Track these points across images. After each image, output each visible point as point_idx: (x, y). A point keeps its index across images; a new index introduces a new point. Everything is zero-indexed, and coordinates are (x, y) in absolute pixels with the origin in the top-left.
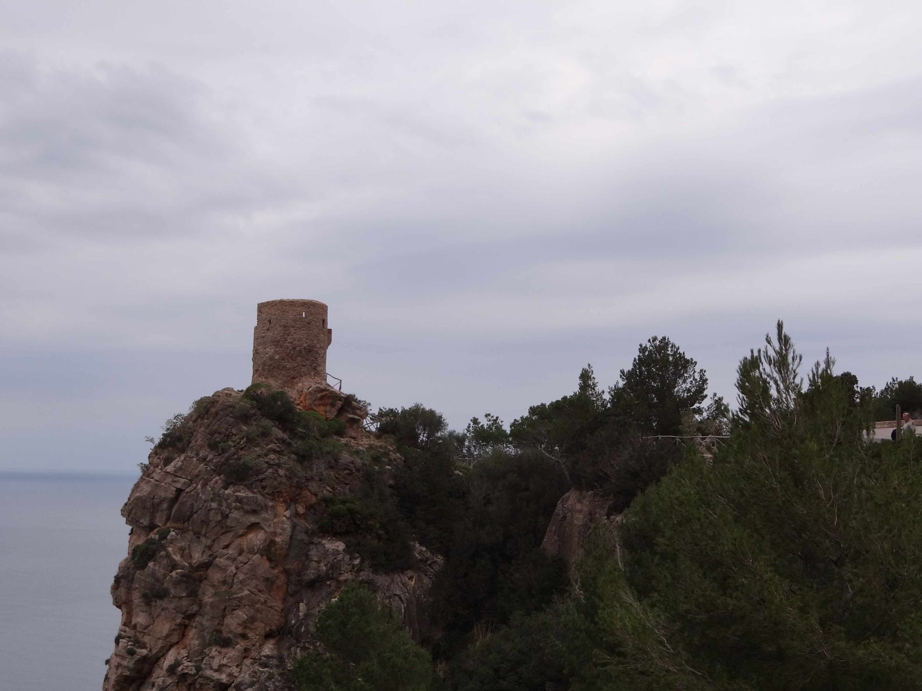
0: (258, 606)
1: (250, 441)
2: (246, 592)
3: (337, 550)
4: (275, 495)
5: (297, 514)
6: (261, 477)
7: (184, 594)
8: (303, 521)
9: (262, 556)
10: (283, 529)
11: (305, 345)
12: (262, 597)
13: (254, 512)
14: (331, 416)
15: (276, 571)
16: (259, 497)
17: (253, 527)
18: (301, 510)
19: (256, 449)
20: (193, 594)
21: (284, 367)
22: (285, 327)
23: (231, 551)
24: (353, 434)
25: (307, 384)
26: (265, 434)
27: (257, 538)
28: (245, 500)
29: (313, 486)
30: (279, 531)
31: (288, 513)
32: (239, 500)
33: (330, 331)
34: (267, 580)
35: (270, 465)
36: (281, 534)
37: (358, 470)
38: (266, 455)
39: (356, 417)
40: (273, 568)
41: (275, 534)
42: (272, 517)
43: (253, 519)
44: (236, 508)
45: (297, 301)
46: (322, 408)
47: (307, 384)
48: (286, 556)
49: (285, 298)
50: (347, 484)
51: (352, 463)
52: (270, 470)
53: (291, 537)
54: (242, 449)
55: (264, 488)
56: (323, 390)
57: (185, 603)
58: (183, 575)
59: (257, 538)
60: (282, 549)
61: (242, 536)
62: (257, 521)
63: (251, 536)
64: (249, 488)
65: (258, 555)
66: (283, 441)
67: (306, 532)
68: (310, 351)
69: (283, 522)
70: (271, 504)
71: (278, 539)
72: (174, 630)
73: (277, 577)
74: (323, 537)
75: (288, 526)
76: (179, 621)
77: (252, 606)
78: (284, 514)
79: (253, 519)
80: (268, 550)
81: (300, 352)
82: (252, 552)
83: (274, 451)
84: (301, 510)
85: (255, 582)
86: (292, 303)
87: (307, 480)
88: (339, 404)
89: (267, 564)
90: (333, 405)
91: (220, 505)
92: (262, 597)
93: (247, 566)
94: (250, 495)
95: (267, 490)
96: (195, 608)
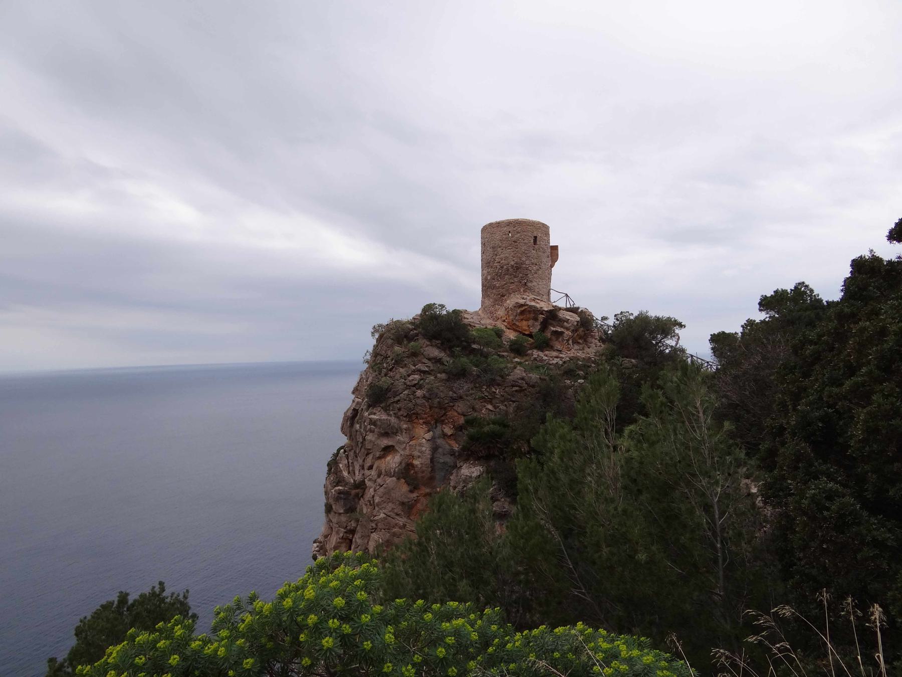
0: (396, 530)
1: (399, 362)
2: (382, 515)
3: (471, 477)
4: (412, 417)
5: (444, 435)
6: (396, 399)
7: (342, 511)
8: (452, 443)
9: (398, 479)
10: (421, 452)
11: (512, 263)
12: (401, 521)
13: (386, 434)
14: (536, 328)
15: (415, 495)
16: (393, 420)
17: (388, 450)
18: (448, 430)
19: (401, 370)
20: (350, 510)
21: (494, 287)
22: (493, 248)
23: (373, 472)
24: (559, 347)
25: (512, 301)
26: (414, 354)
27: (393, 461)
28: (378, 423)
29: (461, 406)
30: (416, 453)
31: (428, 436)
32: (373, 423)
33: (555, 248)
34: (403, 504)
35: (408, 387)
36: (419, 457)
37: (533, 386)
38: (409, 376)
39: (559, 330)
40: (411, 491)
41: (413, 457)
42: (407, 440)
43: (385, 442)
44: (372, 431)
45: (503, 222)
46: (524, 323)
47: (512, 301)
48: (432, 478)
49: (493, 220)
50: (514, 402)
51: (523, 379)
52: (406, 392)
53: (432, 460)
54: (391, 370)
55: (399, 409)
56: (522, 305)
57: (343, 519)
58: (340, 492)
59: (393, 461)
60: (423, 472)
61: (380, 458)
62: (390, 443)
63: (388, 458)
64: (386, 410)
65: (394, 479)
66: (438, 361)
67: (452, 453)
68: (518, 268)
69: (421, 445)
70: (405, 426)
71: (416, 462)
72: (341, 543)
73: (417, 501)
74: (466, 460)
75: (426, 448)
76: (341, 535)
77: (389, 528)
78: (423, 435)
79: (385, 442)
80: (406, 472)
81: (508, 270)
82: (389, 474)
83: (420, 372)
84: (448, 430)
85: (390, 506)
86: (498, 224)
87: (453, 400)
88: (541, 317)
89: (405, 488)
90: (536, 319)
91: (360, 427)
92: (401, 521)
93: (382, 489)
94: (384, 417)
95: (401, 413)
96: (353, 524)
